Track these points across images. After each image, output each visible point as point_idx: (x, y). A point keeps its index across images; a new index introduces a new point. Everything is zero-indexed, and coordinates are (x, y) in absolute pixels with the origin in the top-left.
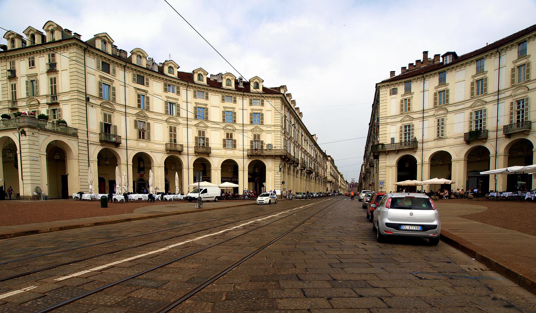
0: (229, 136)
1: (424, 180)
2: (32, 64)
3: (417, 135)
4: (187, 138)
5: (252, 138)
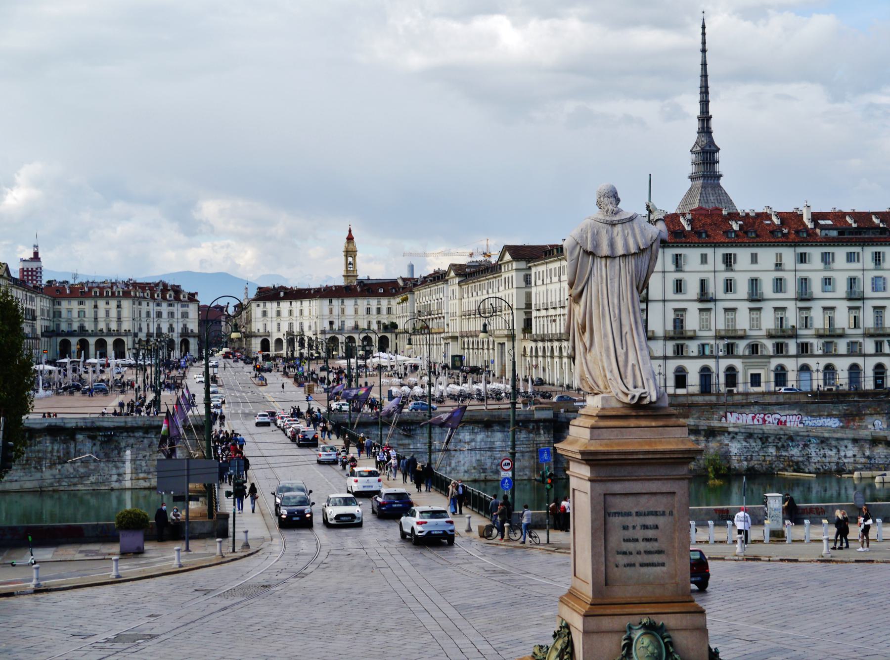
0: (171, 325)
1: (272, 352)
2: (107, 303)
3: (269, 329)
4: (153, 329)
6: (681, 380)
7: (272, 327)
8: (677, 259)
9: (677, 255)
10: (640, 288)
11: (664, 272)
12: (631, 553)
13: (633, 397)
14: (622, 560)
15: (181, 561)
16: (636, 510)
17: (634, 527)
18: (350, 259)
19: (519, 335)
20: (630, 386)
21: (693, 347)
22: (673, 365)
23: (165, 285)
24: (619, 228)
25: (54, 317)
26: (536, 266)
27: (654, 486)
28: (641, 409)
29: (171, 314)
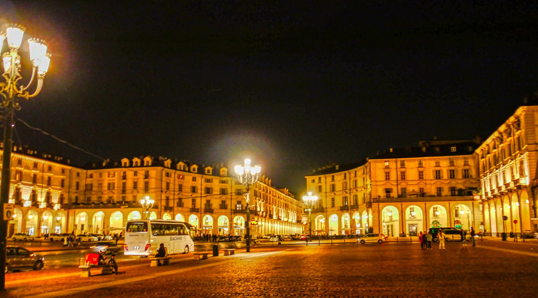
0: (223, 202)
5: (236, 203)
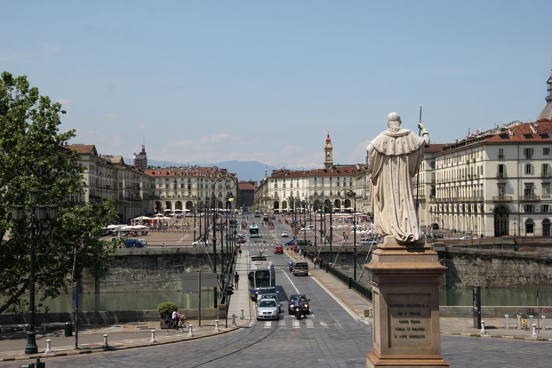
0: (220, 193)
1: (280, 209)
2: (182, 180)
4: (210, 195)
6: (530, 227)
7: (280, 194)
8: (527, 152)
9: (527, 149)
10: (413, 174)
11: (518, 160)
12: (404, 330)
13: (405, 237)
14: (400, 333)
15: (194, 334)
16: (407, 303)
17: (406, 314)
18: (328, 153)
19: (428, 200)
20: (404, 230)
21: (538, 207)
22: (524, 219)
23: (217, 169)
24: (399, 139)
25: (151, 188)
26: (438, 157)
27: (417, 290)
28: (411, 246)
29: (220, 187)
